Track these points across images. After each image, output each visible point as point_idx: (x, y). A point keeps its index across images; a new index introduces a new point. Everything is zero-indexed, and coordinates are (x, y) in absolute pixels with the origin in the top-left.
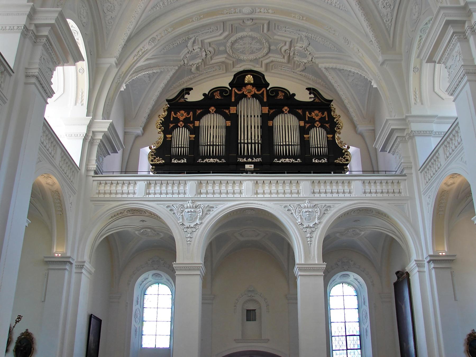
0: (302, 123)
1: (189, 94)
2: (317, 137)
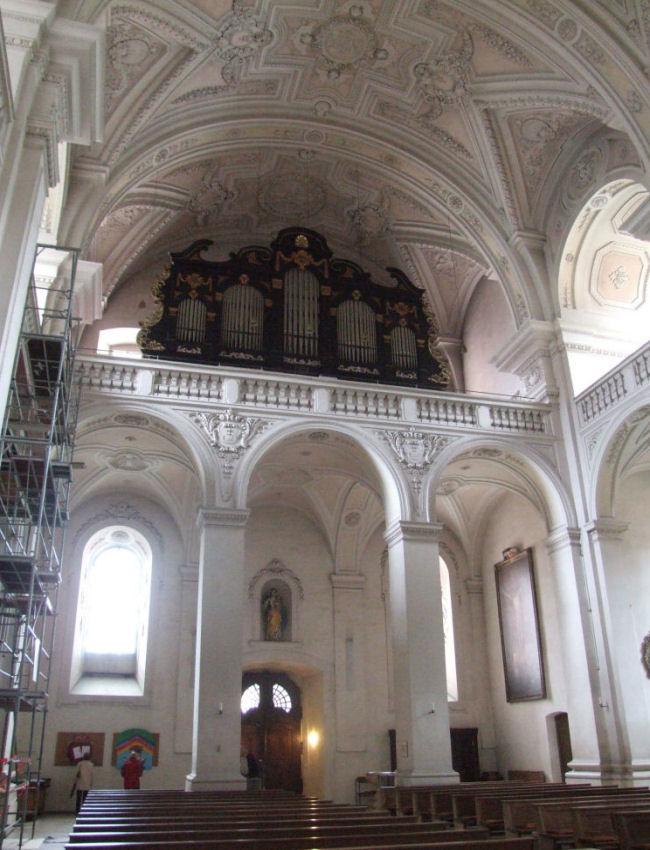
0: (380, 318)
1: (206, 249)
2: (402, 342)
